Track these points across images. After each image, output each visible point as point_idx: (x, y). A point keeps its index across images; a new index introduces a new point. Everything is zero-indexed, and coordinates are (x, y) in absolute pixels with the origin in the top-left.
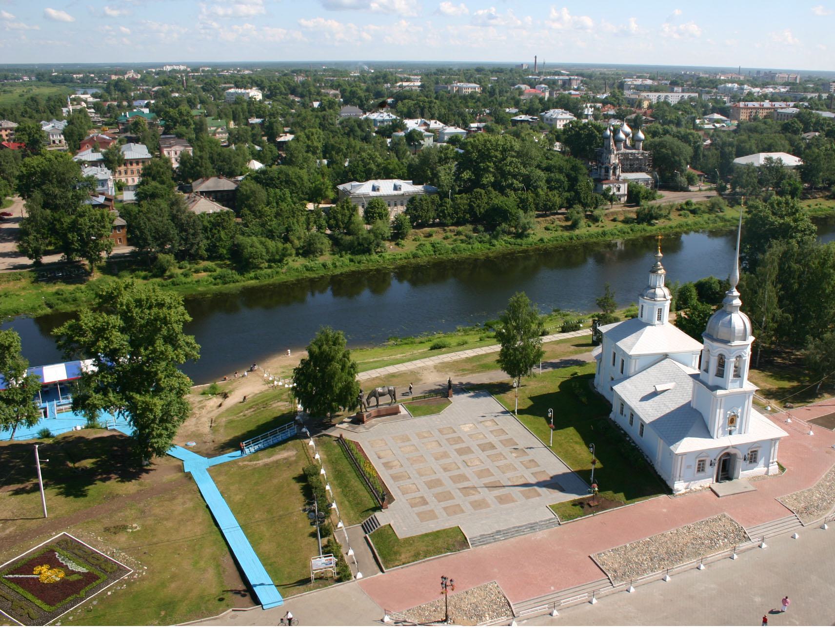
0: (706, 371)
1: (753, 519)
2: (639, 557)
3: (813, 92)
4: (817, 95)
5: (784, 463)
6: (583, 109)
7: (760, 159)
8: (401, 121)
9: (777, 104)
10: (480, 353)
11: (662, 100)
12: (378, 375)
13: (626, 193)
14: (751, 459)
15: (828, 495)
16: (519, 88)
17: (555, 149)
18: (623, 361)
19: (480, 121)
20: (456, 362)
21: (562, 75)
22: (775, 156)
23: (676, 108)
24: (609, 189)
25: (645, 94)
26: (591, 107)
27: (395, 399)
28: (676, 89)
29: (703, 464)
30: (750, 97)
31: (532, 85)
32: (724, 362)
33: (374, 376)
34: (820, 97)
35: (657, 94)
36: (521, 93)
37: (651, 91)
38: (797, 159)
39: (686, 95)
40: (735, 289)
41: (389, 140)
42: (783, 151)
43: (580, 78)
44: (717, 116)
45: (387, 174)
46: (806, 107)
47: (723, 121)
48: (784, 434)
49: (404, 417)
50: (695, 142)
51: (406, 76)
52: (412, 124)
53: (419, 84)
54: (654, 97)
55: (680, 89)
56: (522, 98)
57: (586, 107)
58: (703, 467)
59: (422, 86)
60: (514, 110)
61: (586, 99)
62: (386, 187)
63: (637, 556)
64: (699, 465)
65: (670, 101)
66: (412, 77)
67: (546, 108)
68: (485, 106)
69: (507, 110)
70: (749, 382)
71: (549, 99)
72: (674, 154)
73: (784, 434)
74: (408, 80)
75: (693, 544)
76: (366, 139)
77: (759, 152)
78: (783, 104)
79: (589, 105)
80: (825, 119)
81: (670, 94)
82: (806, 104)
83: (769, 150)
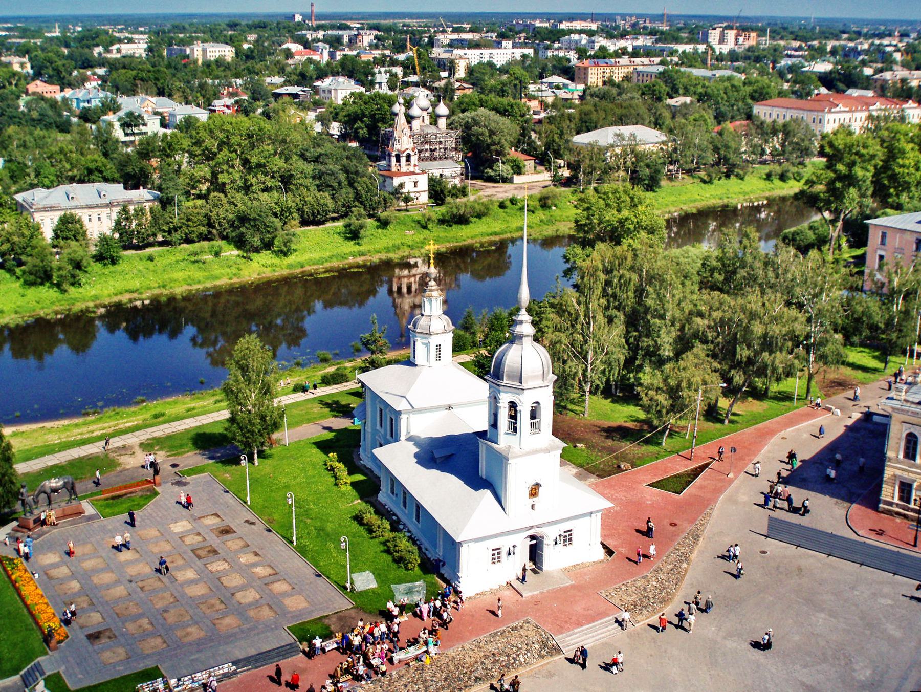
0: (494, 425)
1: (566, 622)
2: (409, 687)
3: (686, 43)
4: (692, 46)
5: (611, 544)
6: (373, 75)
7: (604, 136)
8: (114, 101)
9: (637, 60)
10: (205, 422)
11: (485, 60)
12: (57, 462)
13: (426, 188)
14: (565, 541)
15: (668, 581)
16: (288, 49)
17: (331, 132)
18: (392, 420)
19: (231, 95)
20: (169, 437)
21: (350, 28)
22: (626, 130)
23: (504, 70)
24: (401, 186)
25: (458, 52)
26: (386, 72)
27: (75, 494)
28: (504, 43)
29: (499, 553)
30: (603, 54)
31: (306, 45)
32: (516, 412)
33: (50, 464)
34: (696, 50)
35: (477, 52)
36: (289, 54)
37: (469, 48)
38: (657, 132)
39: (518, 53)
40: (523, 311)
41: (94, 127)
42: (643, 124)
43: (375, 32)
44: (556, 79)
45: (87, 176)
46: (677, 64)
47: (565, 86)
48: (608, 504)
49: (90, 518)
50: (523, 116)
51: (127, 35)
52: (128, 103)
53: (146, 46)
54: (474, 56)
55: (510, 43)
56: (290, 62)
57: (380, 72)
58: (499, 558)
59: (150, 50)
60: (278, 80)
61: (381, 62)
62: (84, 193)
63: (406, 686)
64: (493, 555)
65: (495, 61)
66: (136, 36)
67: (322, 75)
68: (237, 76)
69: (268, 80)
70: (554, 437)
71: (328, 64)
72: (492, 133)
73: (608, 504)
74: (131, 41)
75: (482, 663)
76: (64, 127)
77: (612, 125)
78: (646, 60)
79: (383, 69)
80: (697, 78)
81: (495, 51)
82: (676, 59)
83: (621, 121)
